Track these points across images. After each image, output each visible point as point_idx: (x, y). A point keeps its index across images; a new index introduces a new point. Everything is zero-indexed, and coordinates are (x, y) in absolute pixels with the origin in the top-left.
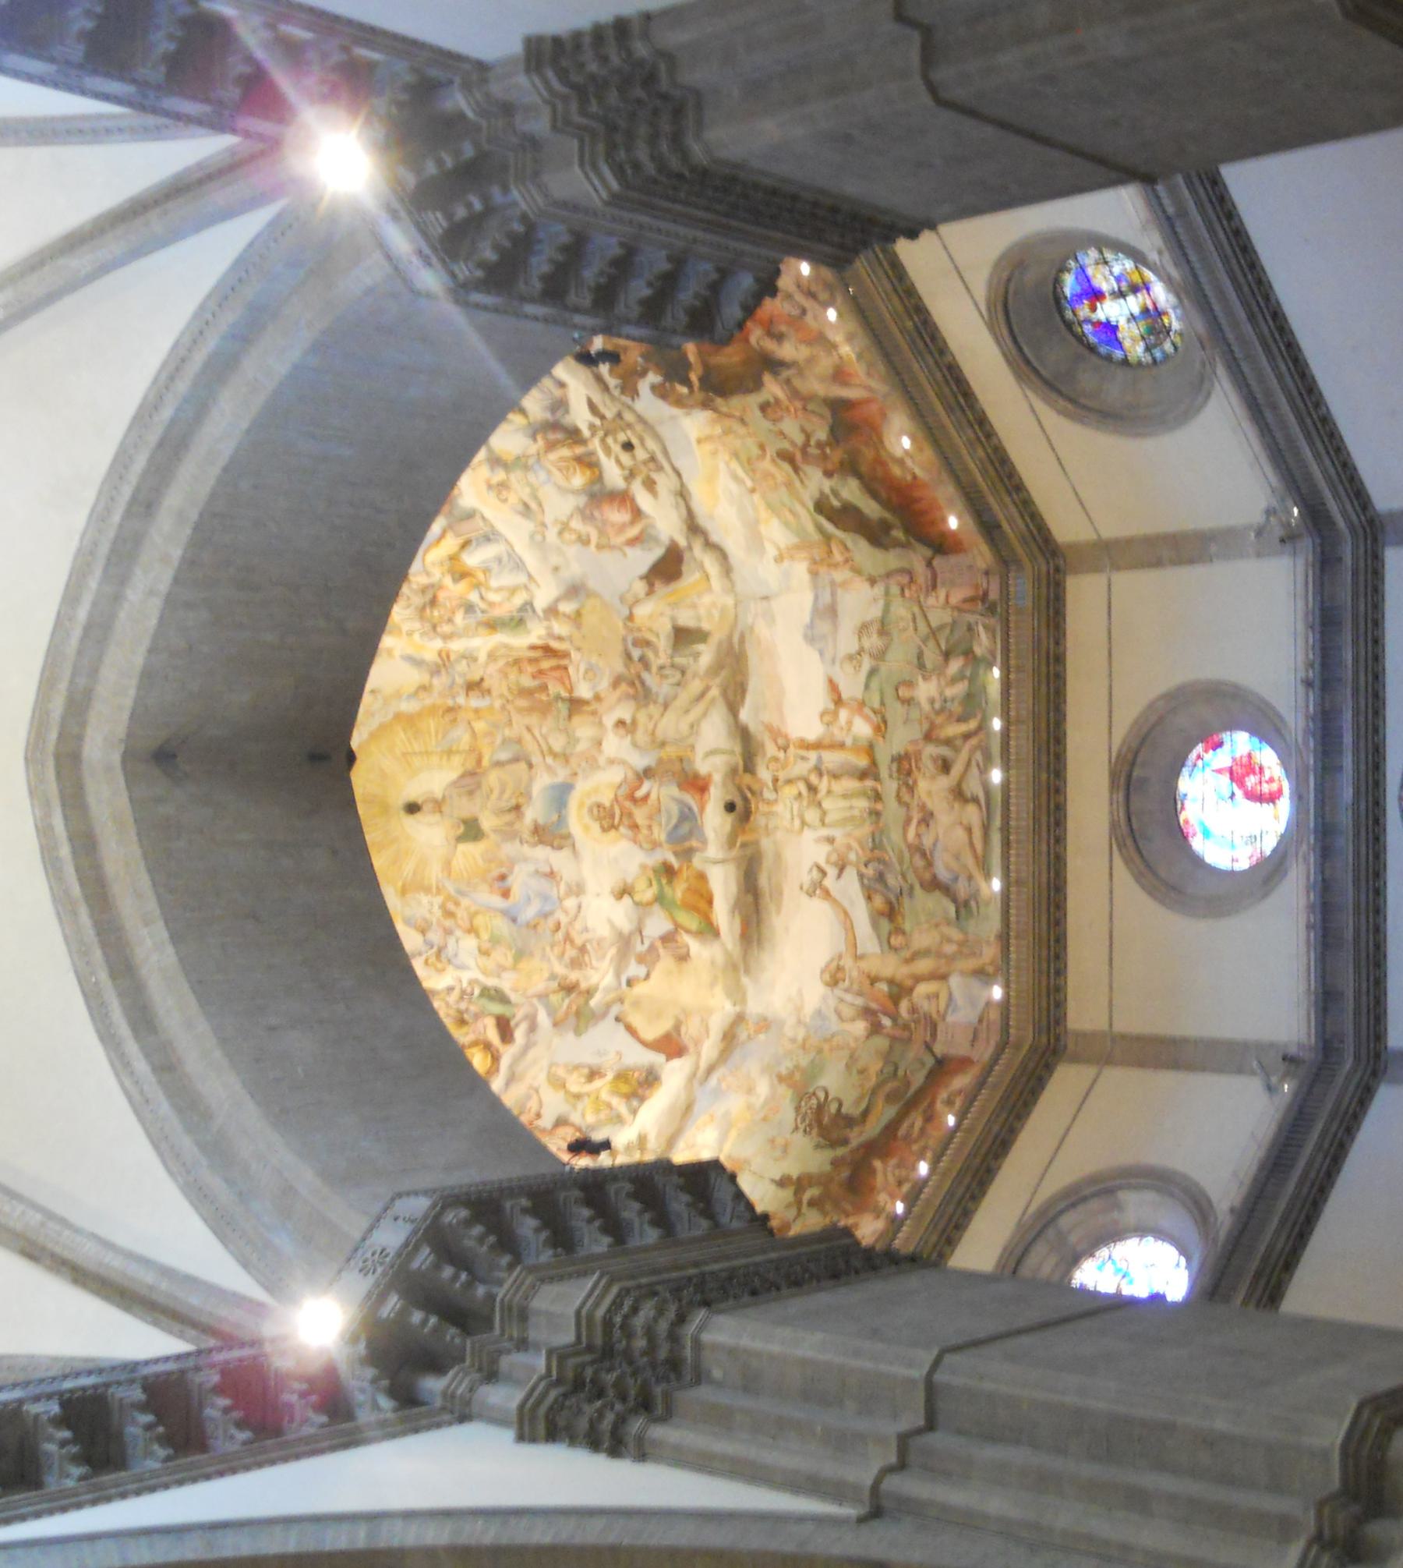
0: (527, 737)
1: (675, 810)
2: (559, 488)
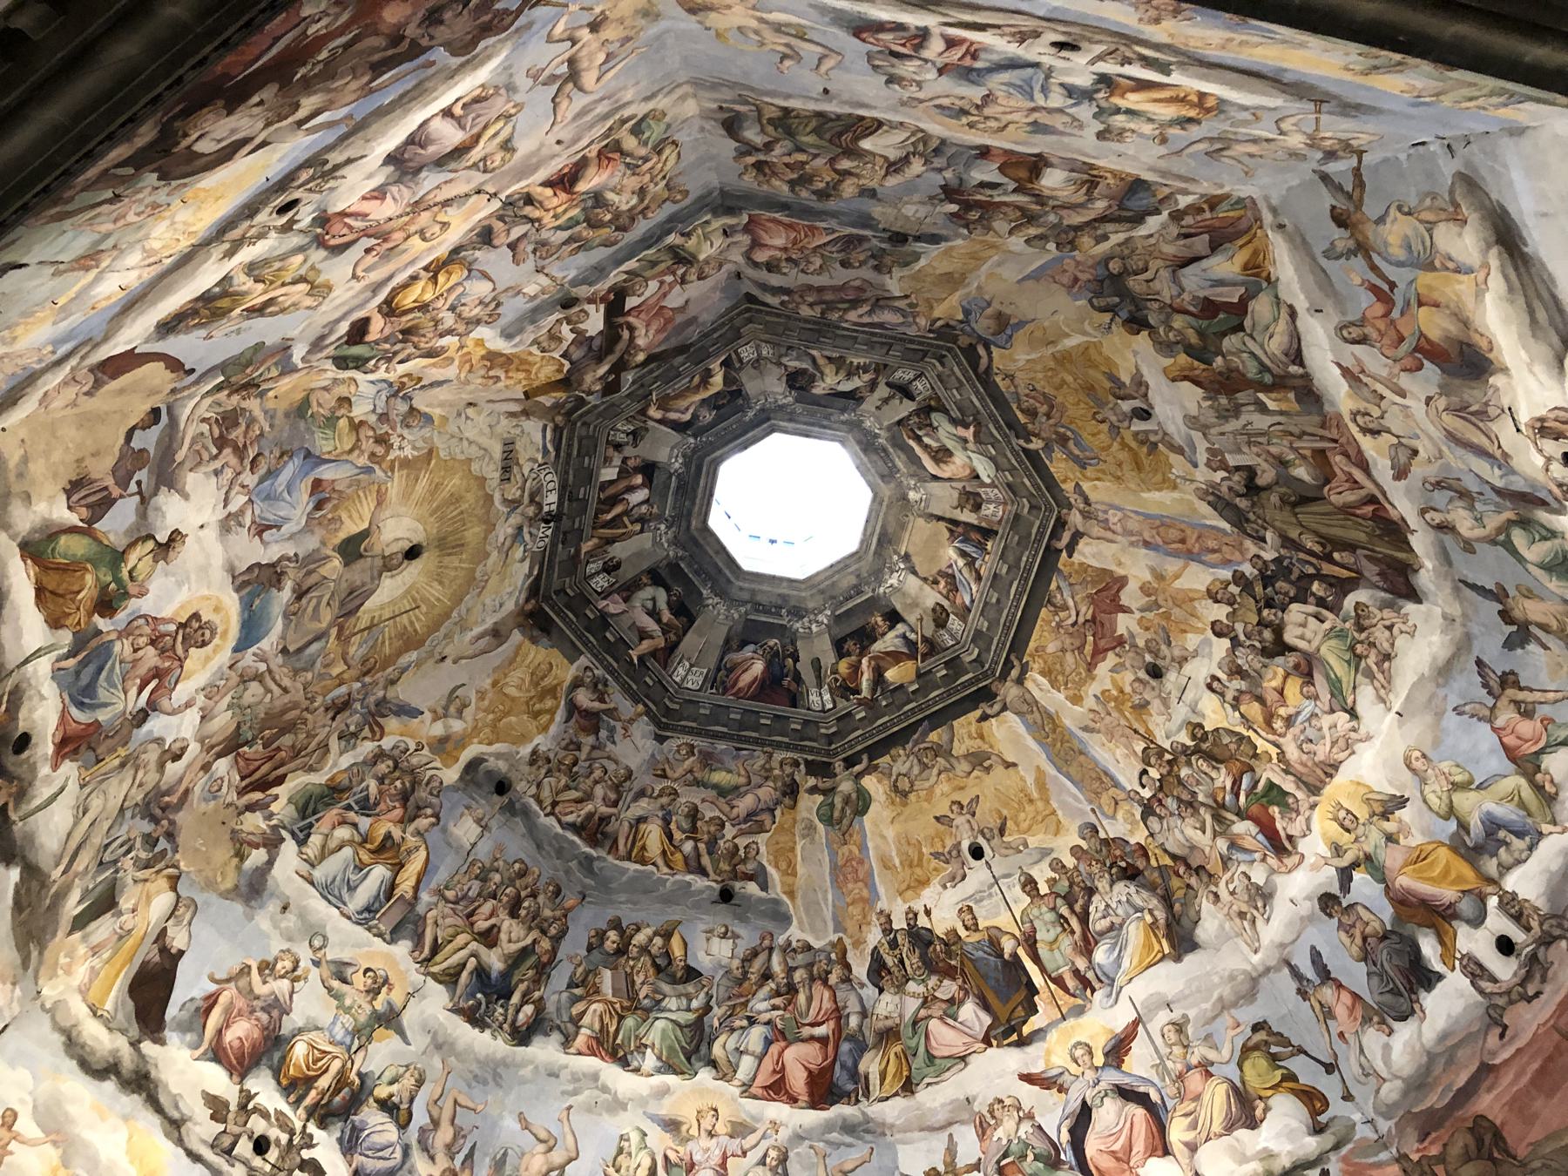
0: (286, 682)
1: (102, 694)
2: (317, 1028)
